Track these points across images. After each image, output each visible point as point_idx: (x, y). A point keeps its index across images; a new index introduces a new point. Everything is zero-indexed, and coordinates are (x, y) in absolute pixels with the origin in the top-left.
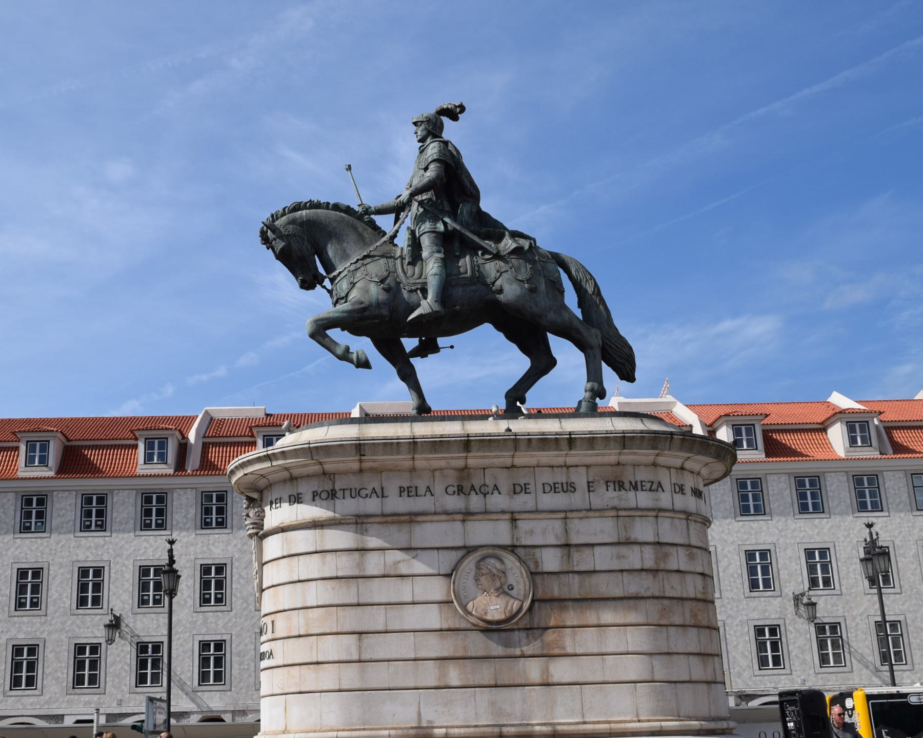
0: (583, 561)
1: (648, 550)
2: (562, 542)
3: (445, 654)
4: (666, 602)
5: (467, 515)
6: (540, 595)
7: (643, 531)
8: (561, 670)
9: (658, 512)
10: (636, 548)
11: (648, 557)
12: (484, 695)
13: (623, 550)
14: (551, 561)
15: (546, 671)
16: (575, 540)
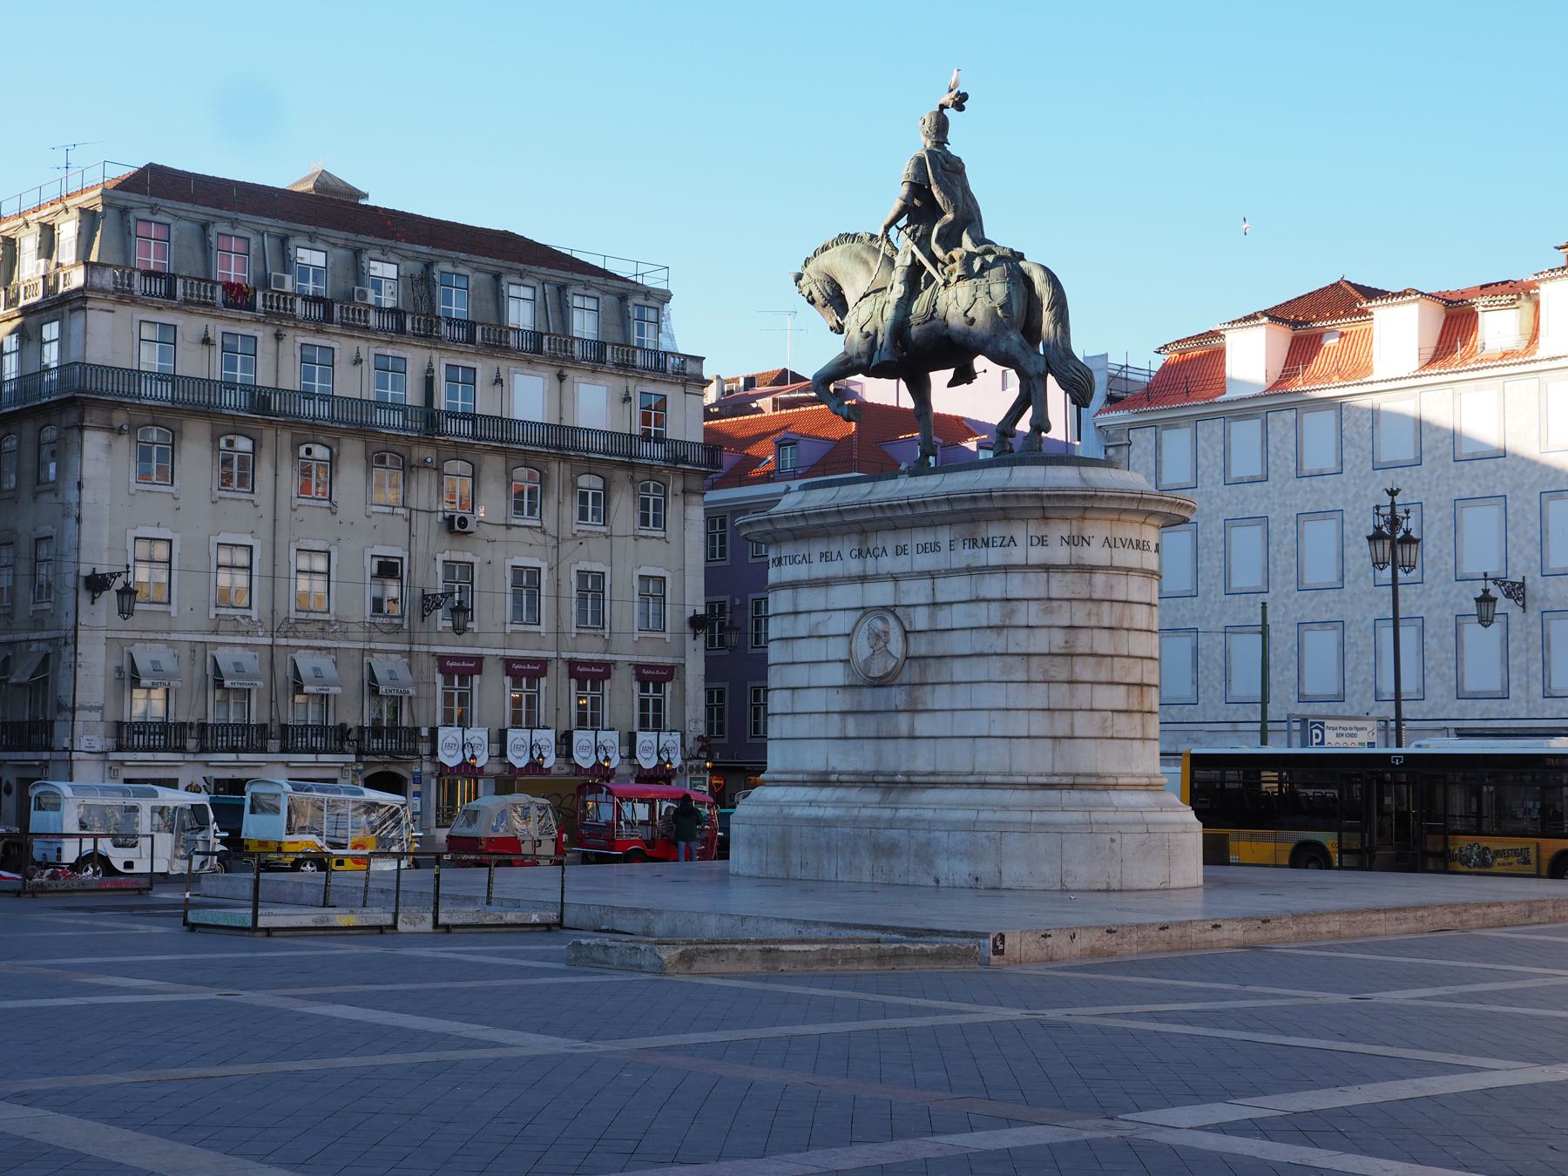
0: (945, 618)
1: (994, 606)
2: (930, 600)
3: (845, 708)
4: (1008, 659)
5: (863, 579)
6: (911, 653)
7: (993, 586)
8: (924, 725)
9: (1006, 569)
10: (984, 605)
11: (994, 614)
12: (869, 746)
13: (972, 607)
14: (921, 620)
15: (912, 726)
16: (940, 599)
